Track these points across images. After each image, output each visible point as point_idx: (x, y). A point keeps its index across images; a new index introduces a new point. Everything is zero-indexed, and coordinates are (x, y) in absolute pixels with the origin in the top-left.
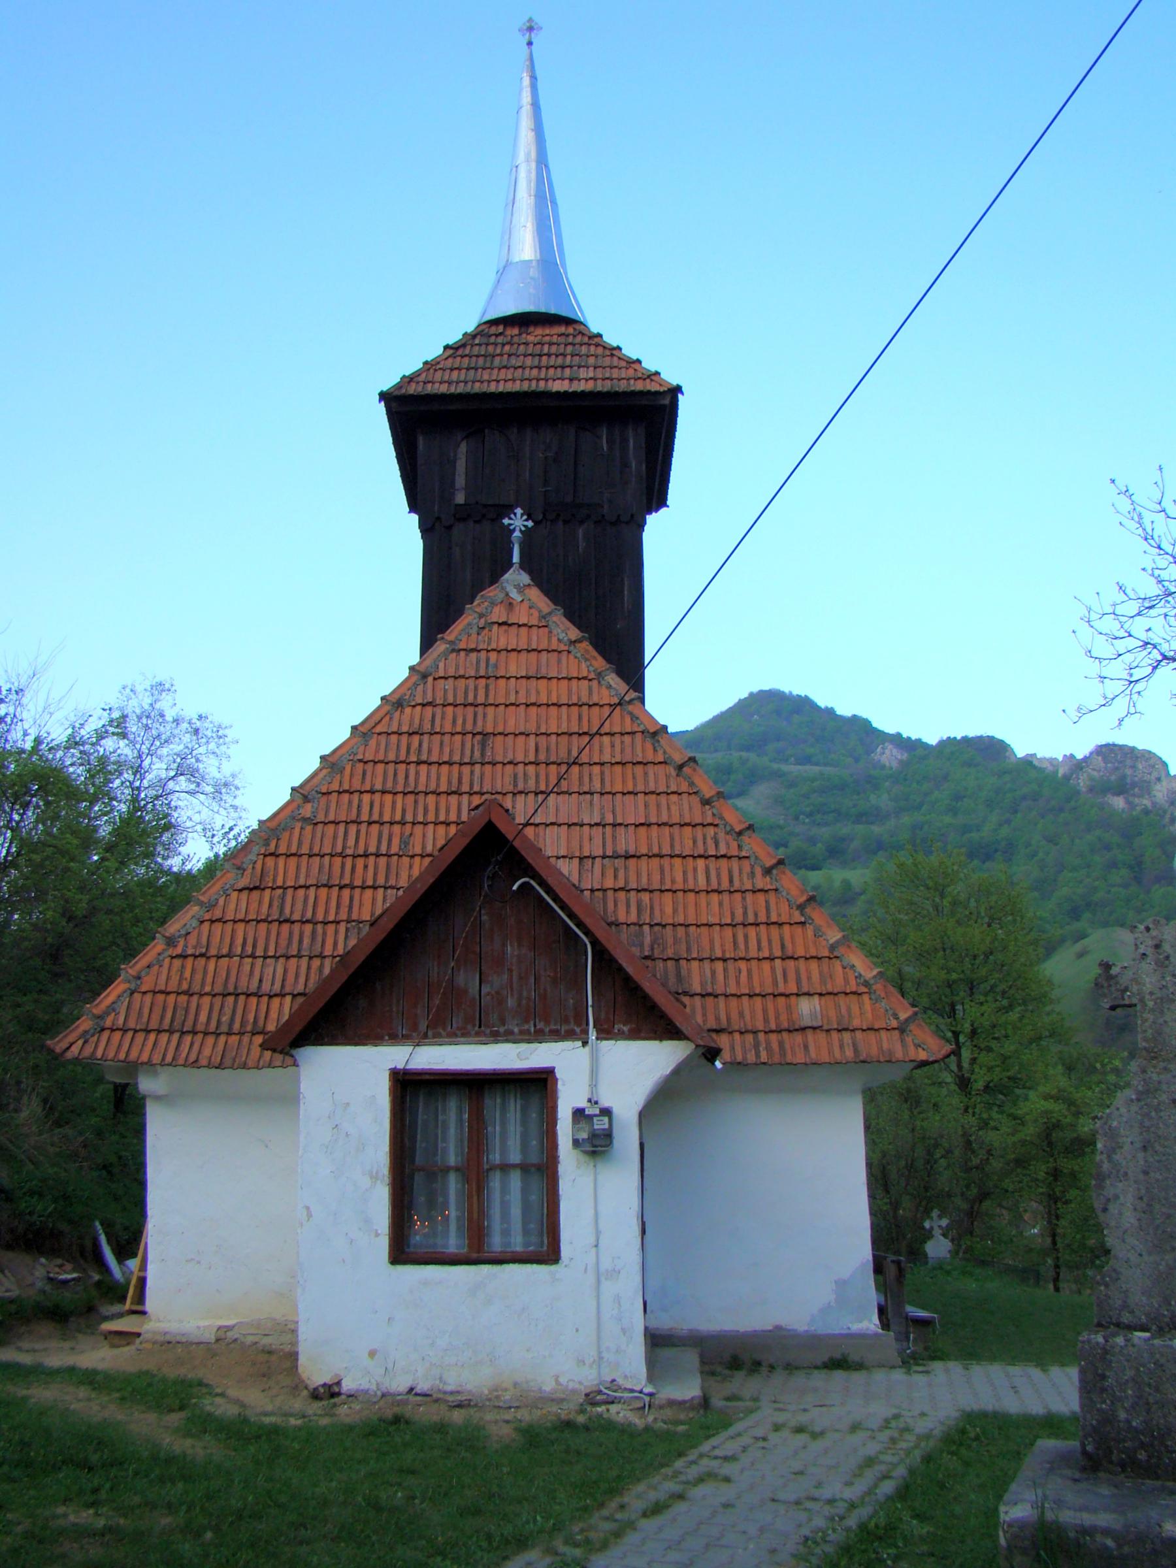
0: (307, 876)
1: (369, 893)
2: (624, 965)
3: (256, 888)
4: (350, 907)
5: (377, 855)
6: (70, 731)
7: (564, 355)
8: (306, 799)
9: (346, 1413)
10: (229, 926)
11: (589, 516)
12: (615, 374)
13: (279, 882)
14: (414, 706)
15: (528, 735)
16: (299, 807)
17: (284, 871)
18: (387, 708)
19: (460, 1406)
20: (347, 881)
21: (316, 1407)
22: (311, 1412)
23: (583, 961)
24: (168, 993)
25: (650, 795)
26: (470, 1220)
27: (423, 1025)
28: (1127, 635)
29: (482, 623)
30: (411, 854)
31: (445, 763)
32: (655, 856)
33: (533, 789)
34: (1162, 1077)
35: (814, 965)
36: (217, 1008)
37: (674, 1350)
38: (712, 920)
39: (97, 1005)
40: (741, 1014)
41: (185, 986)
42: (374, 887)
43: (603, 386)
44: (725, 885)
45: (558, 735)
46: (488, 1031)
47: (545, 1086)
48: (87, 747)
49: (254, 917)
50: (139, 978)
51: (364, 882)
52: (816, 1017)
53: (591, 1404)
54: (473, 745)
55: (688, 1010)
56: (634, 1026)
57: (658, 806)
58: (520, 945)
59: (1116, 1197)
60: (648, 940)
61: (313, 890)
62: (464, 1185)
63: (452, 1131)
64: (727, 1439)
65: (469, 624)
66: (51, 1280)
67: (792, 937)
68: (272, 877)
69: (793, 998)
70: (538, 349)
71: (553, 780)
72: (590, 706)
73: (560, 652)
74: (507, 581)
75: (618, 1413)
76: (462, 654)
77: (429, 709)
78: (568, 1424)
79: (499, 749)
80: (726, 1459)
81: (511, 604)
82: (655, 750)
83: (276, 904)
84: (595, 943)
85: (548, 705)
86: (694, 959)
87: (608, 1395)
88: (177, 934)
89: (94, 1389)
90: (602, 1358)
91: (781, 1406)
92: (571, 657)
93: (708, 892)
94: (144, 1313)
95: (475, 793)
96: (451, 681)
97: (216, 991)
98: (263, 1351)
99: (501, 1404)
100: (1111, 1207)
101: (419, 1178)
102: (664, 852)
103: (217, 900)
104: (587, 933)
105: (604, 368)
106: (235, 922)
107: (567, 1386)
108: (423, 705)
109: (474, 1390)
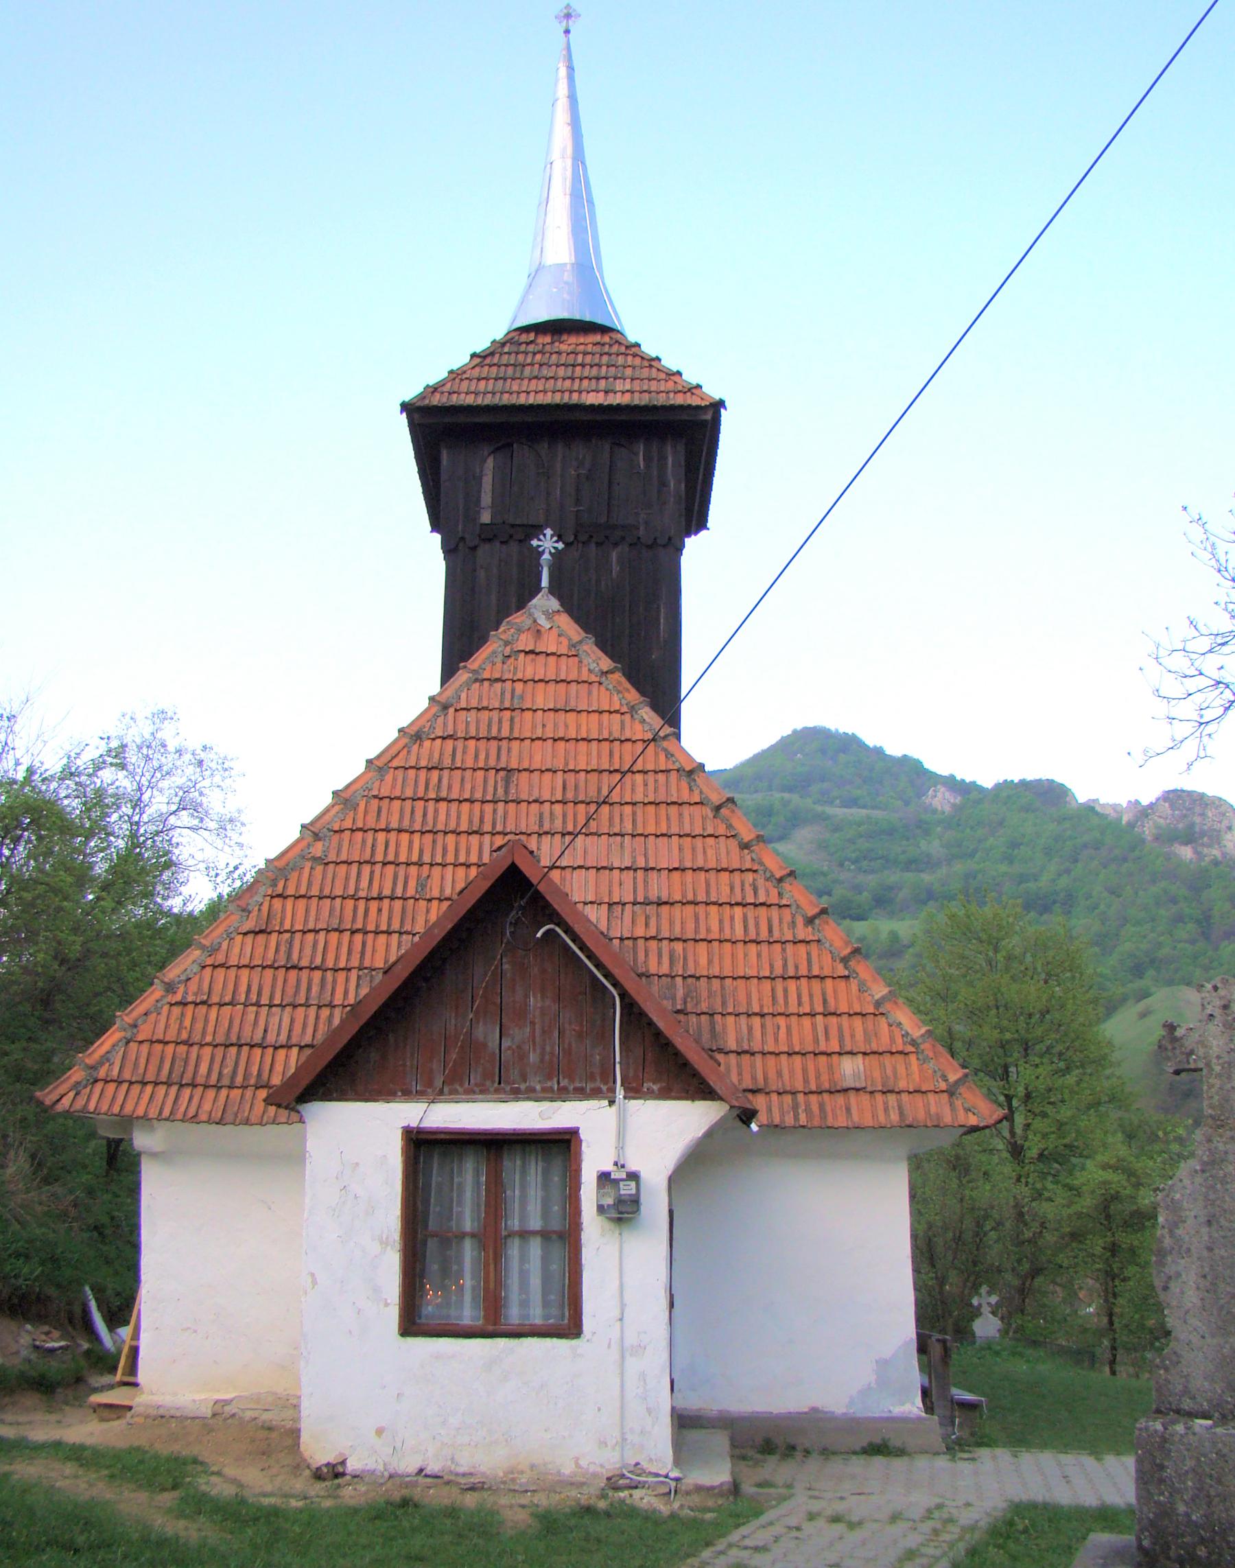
0: (317, 919)
1: (382, 938)
2: (655, 1019)
3: (261, 932)
4: (363, 953)
5: (392, 898)
6: (65, 761)
7: (599, 366)
8: (317, 837)
9: (350, 1494)
10: (233, 971)
11: (623, 538)
12: (654, 386)
13: (287, 926)
14: (433, 739)
15: (555, 772)
16: (309, 846)
17: (292, 914)
18: (405, 740)
19: (472, 1488)
20: (359, 925)
21: (319, 1488)
22: (313, 1493)
23: (611, 1014)
24: (167, 1043)
25: (685, 838)
26: (486, 1289)
27: (438, 1082)
28: (1197, 673)
29: (507, 651)
30: (428, 897)
31: (466, 800)
32: (689, 903)
33: (560, 830)
34: (1228, 1146)
35: (857, 1022)
36: (218, 1059)
37: (704, 1431)
38: (750, 973)
39: (90, 1054)
40: (779, 1074)
41: (184, 1036)
42: (389, 933)
43: (640, 399)
44: (764, 935)
45: (587, 772)
46: (508, 1088)
47: (569, 1148)
48: (83, 778)
49: (260, 963)
50: (135, 1026)
51: (377, 926)
52: (859, 1078)
53: (613, 1489)
54: (496, 782)
55: (722, 1068)
56: (664, 1084)
57: (694, 849)
58: (543, 997)
59: (1178, 1275)
60: (680, 993)
61: (322, 934)
62: (480, 1253)
63: (468, 1195)
64: (758, 1528)
65: (494, 652)
66: (37, 1347)
67: (835, 991)
68: (279, 920)
69: (835, 1057)
70: (571, 358)
71: (582, 821)
72: (622, 741)
73: (590, 683)
74: (535, 607)
75: (642, 1499)
76: (486, 684)
77: (450, 743)
78: (589, 1510)
79: (524, 786)
80: (756, 1549)
81: (538, 631)
82: (691, 790)
83: (283, 949)
84: (624, 995)
85: (577, 740)
86: (729, 1014)
87: (631, 1479)
88: (177, 980)
89: (81, 1465)
90: (626, 1439)
91: (816, 1493)
92: (602, 688)
93: (745, 942)
94: (136, 1385)
95: (498, 833)
96: (474, 712)
97: (217, 1041)
98: (263, 1427)
99: (517, 1487)
100: (1172, 1285)
101: (432, 1244)
102: (699, 899)
103: (220, 943)
104: (616, 984)
105: (642, 380)
106: (239, 967)
107: (588, 1469)
108: (444, 738)
109: (488, 1473)
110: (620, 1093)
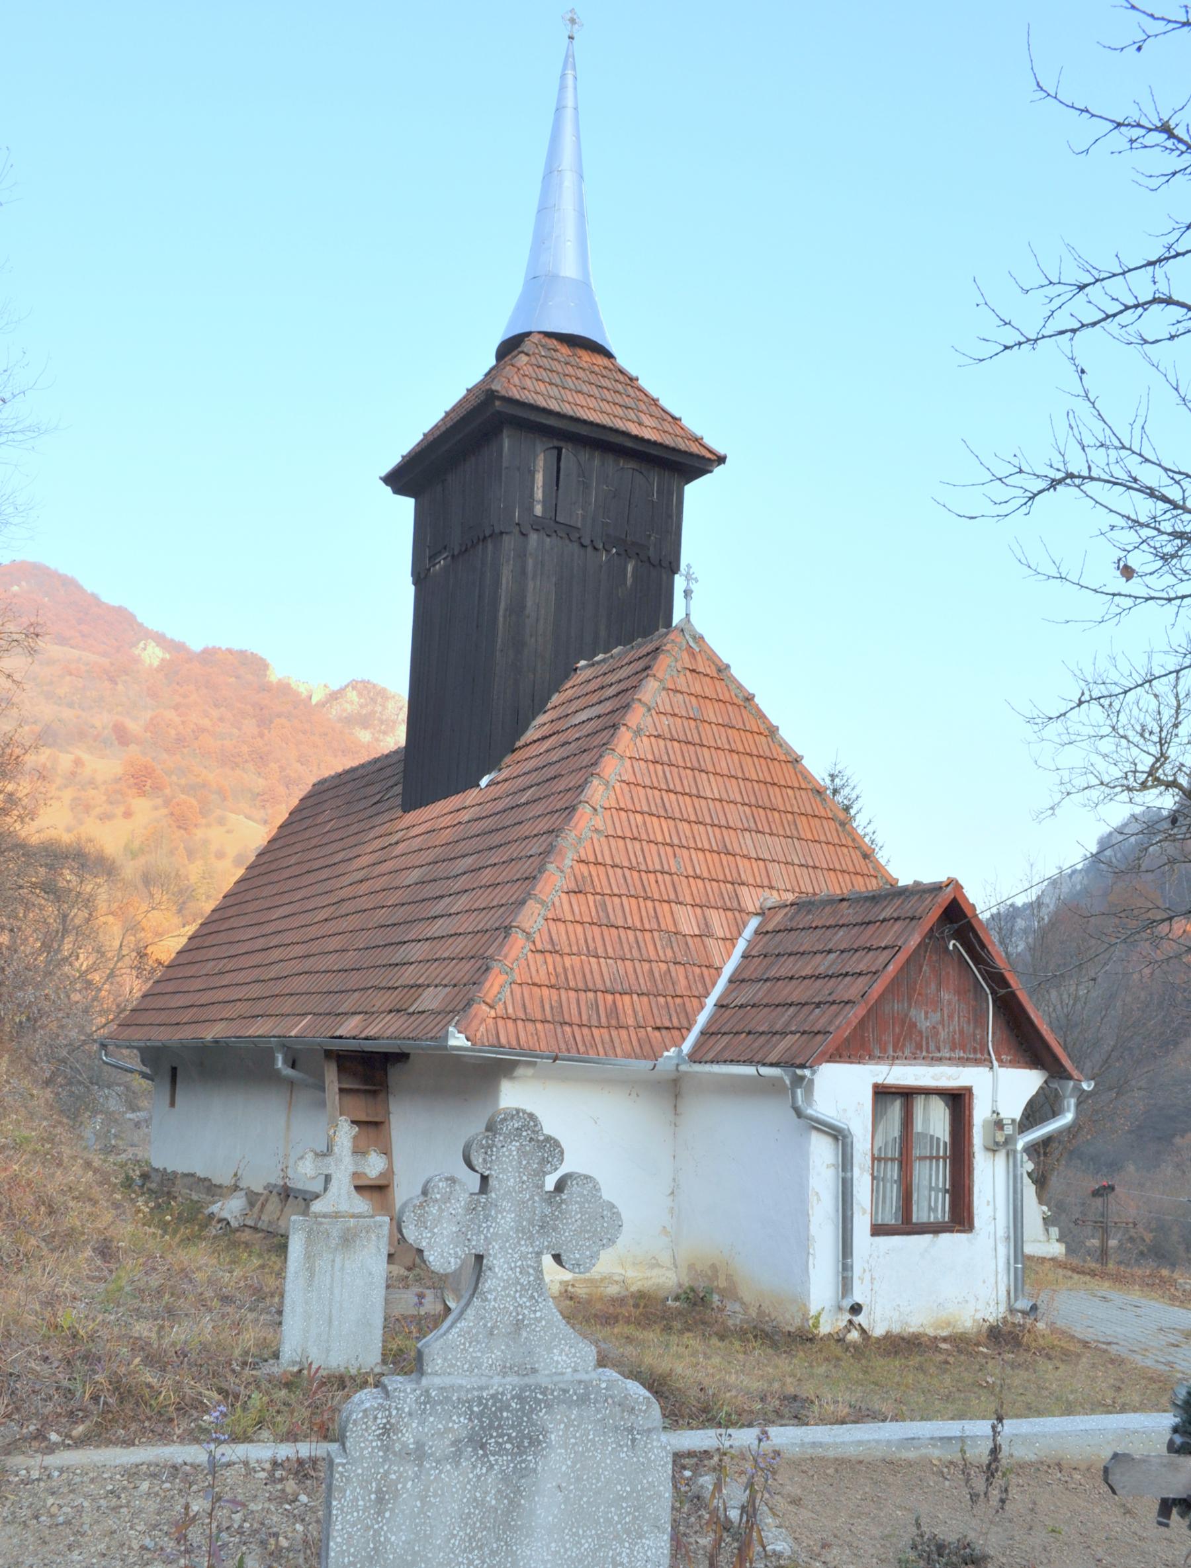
23: (985, 1006)
110: (995, 1063)
